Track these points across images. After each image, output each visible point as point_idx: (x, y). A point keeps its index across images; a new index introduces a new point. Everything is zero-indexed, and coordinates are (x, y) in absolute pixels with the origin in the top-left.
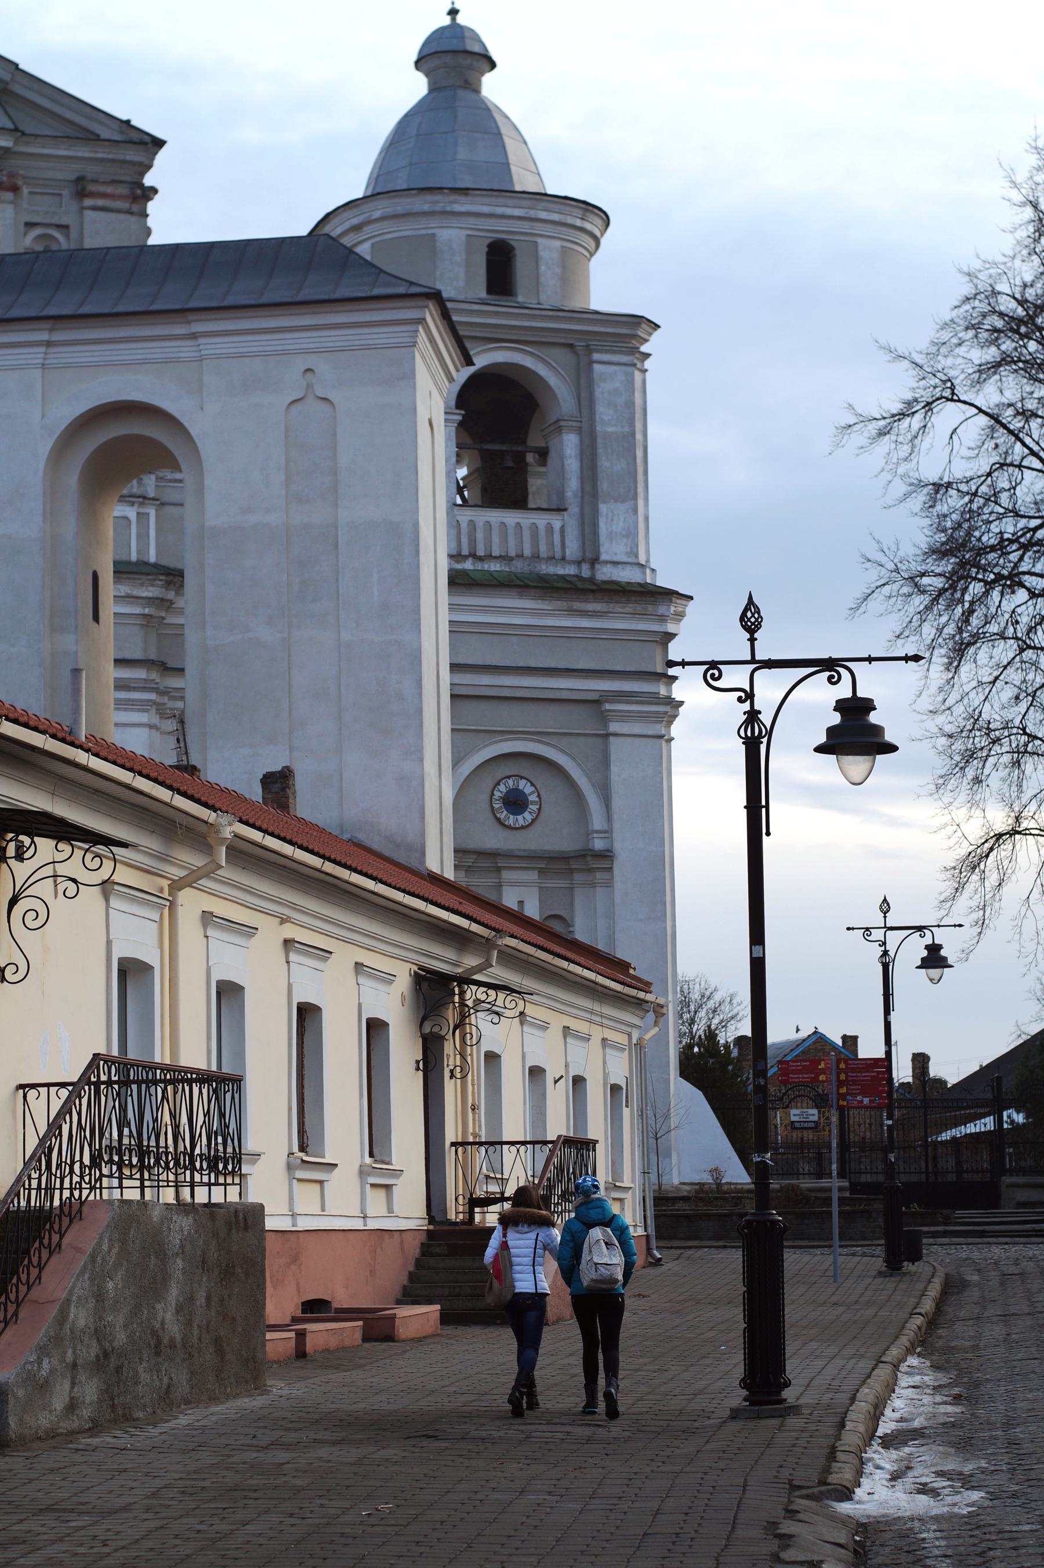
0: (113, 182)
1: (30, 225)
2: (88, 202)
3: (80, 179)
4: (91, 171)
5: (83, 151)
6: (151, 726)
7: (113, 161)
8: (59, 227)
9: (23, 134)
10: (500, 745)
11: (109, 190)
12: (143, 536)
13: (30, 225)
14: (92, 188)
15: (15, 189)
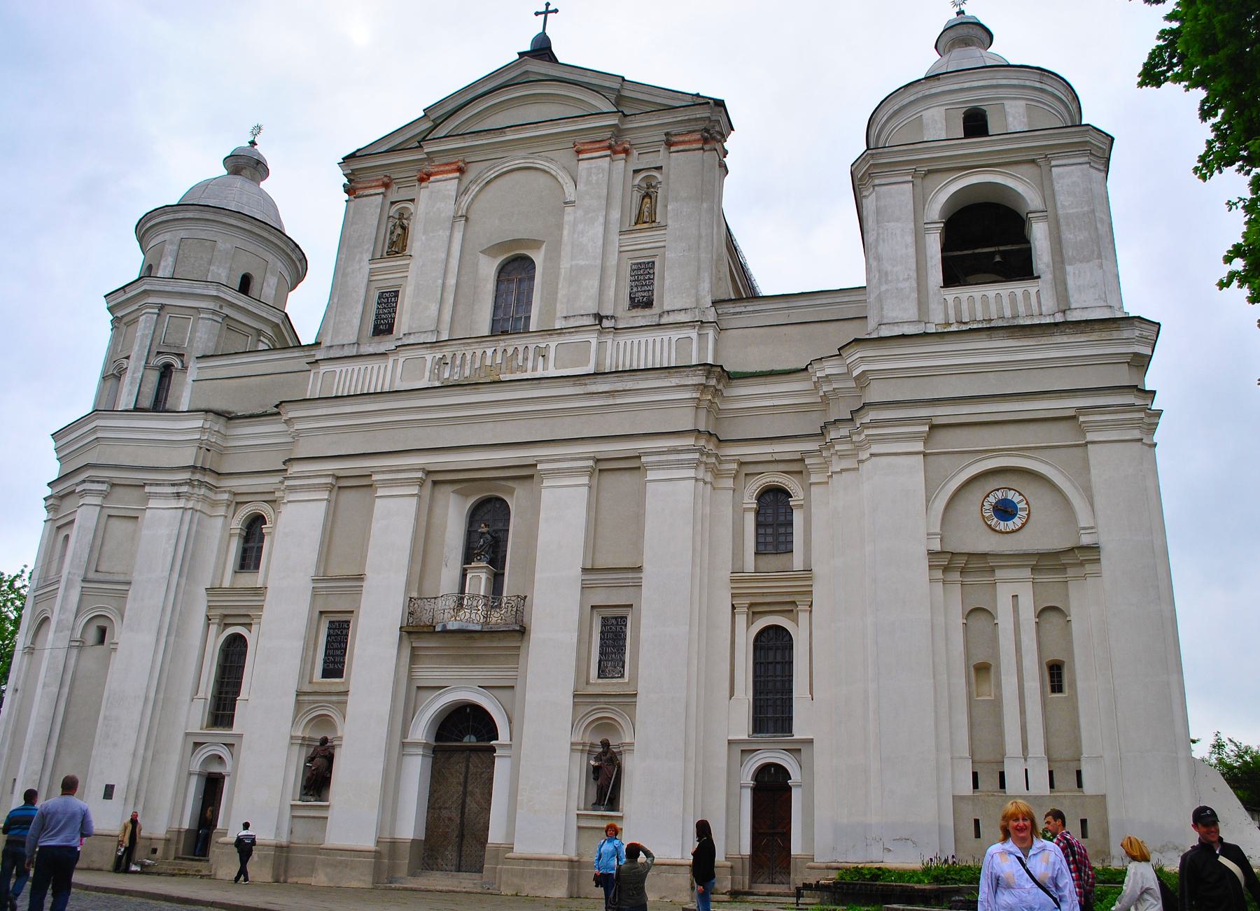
0: (690, 132)
1: (636, 172)
2: (673, 149)
3: (667, 134)
4: (674, 130)
5: (668, 118)
6: (697, 480)
7: (689, 120)
8: (656, 168)
9: (625, 116)
10: (993, 460)
11: (686, 138)
12: (702, 349)
13: (636, 172)
14: (675, 139)
15: (626, 151)
